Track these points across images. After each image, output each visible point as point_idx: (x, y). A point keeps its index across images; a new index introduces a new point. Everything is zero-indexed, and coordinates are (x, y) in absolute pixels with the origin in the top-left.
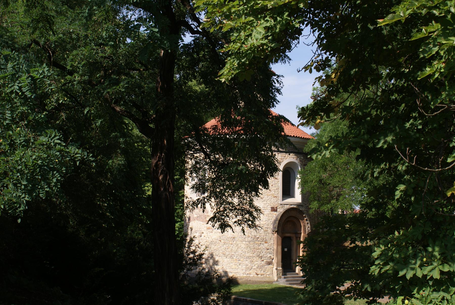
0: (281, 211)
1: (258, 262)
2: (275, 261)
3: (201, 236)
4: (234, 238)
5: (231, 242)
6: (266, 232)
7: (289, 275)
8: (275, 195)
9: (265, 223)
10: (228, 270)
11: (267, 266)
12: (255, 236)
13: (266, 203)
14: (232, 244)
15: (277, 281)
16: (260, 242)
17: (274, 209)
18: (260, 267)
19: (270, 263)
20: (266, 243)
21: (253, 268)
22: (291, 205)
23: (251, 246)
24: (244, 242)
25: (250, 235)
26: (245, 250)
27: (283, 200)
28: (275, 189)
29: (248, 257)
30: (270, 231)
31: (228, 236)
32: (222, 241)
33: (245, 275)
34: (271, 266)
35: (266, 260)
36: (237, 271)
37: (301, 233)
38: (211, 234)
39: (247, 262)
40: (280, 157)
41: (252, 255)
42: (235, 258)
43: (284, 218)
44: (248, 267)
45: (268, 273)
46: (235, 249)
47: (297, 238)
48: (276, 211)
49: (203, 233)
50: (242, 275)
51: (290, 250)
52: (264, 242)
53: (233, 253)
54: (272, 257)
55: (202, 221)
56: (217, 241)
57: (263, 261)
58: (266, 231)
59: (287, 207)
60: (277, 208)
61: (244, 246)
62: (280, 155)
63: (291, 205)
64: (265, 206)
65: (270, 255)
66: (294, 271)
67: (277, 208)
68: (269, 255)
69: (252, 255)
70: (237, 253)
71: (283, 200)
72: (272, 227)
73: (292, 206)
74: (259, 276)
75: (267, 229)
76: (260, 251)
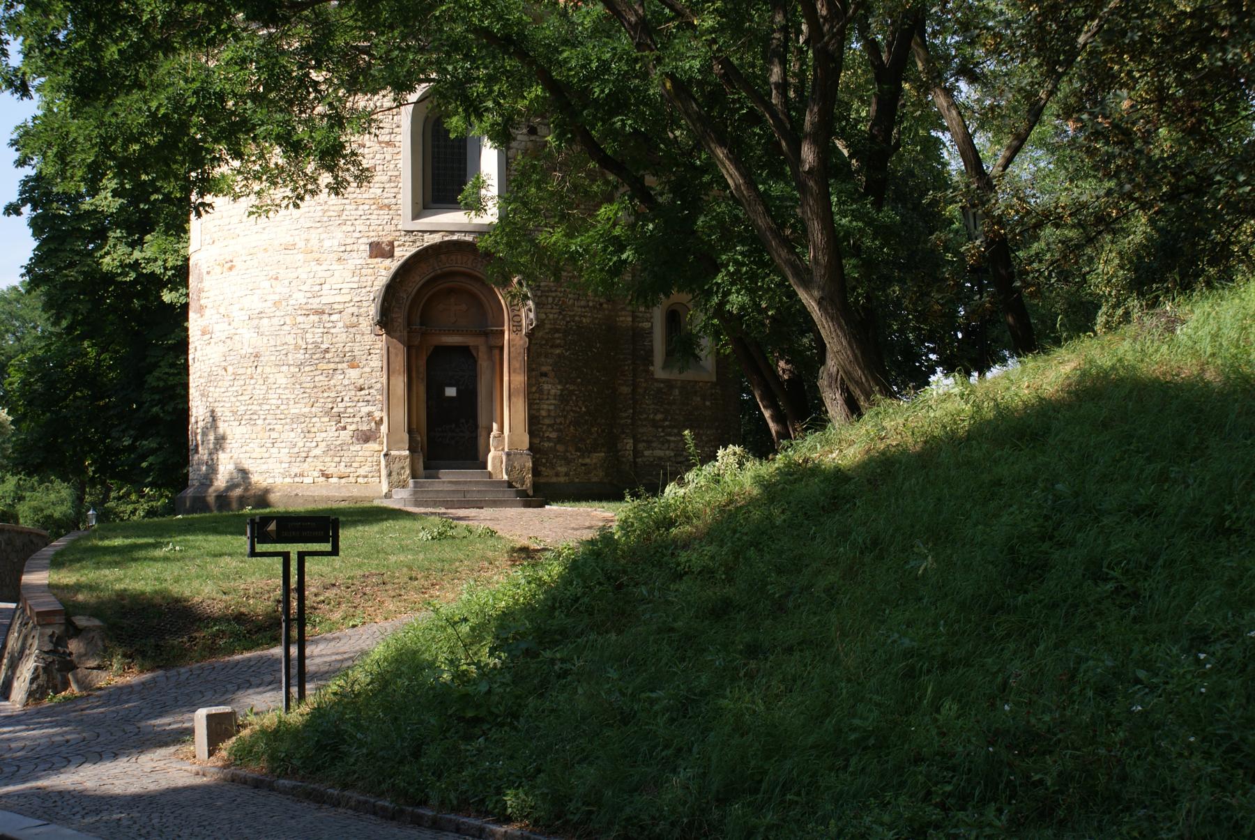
0: (404, 252)
1: (330, 433)
2: (384, 428)
7: (449, 478)
8: (386, 201)
9: (348, 298)
10: (247, 465)
11: (358, 447)
13: (352, 229)
15: (388, 496)
16: (332, 366)
17: (380, 250)
18: (336, 451)
19: (366, 437)
21: (312, 454)
22: (453, 233)
23: (303, 379)
24: (285, 368)
26: (287, 394)
27: (416, 216)
28: (385, 178)
29: (296, 419)
31: (243, 352)
32: (230, 369)
33: (288, 480)
34: (373, 446)
35: (354, 427)
36: (264, 467)
37: (502, 332)
39: (292, 435)
41: (307, 410)
42: (260, 422)
43: (417, 281)
44: (296, 450)
45: (362, 472)
46: (259, 392)
47: (491, 348)
48: (391, 255)
50: (279, 480)
51: (469, 398)
53: (255, 407)
57: (344, 428)
59: (431, 239)
60: (391, 244)
63: (453, 233)
64: (349, 241)
65: (370, 408)
66: (485, 468)
67: (391, 244)
69: (307, 410)
70: (265, 407)
71: (413, 219)
73: (455, 237)
76: (333, 395)
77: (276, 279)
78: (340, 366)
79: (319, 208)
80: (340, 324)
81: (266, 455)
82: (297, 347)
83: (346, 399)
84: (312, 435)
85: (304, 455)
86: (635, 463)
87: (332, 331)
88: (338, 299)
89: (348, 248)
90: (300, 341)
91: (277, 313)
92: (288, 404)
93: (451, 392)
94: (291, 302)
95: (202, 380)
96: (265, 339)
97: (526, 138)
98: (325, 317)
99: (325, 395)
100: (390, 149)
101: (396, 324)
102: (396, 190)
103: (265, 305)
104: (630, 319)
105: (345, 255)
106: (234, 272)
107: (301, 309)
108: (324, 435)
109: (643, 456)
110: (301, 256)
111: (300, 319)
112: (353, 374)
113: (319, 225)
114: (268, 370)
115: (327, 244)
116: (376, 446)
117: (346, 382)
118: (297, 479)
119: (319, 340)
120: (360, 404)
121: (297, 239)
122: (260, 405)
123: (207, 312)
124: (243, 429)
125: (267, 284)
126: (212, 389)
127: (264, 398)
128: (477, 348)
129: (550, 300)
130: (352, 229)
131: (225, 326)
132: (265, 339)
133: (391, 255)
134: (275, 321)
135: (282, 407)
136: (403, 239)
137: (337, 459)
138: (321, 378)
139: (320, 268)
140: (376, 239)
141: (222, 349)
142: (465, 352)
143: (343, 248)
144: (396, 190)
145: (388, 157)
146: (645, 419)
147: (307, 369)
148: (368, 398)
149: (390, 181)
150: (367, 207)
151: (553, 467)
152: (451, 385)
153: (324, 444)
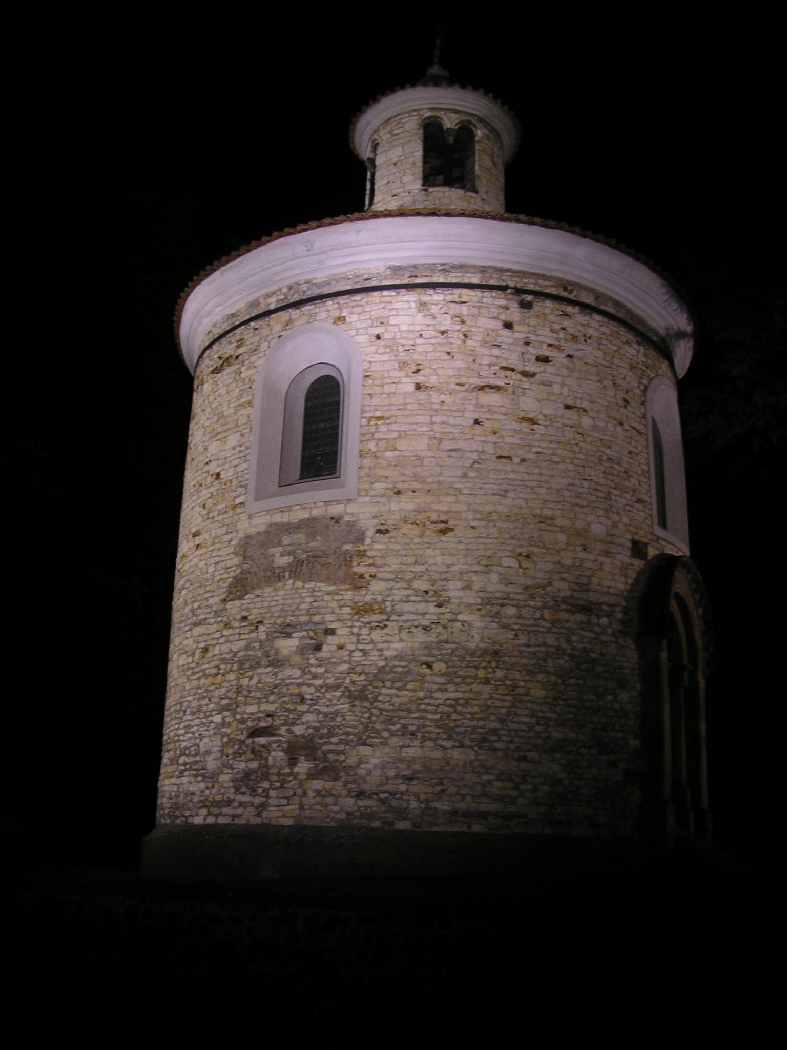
3: (318, 648)
4: (496, 653)
5: (481, 673)
12: (585, 650)
14: (487, 681)
24: (540, 677)
25: (564, 645)
32: (439, 667)
36: (511, 809)
38: (376, 635)
41: (572, 736)
49: (332, 632)
53: (492, 725)
55: (328, 580)
56: (412, 666)
61: (542, 693)
77: (528, 557)
78: (610, 684)
79: (585, 484)
80: (609, 631)
81: (514, 793)
82: (560, 651)
87: (604, 638)
88: (606, 599)
90: (564, 645)
91: (532, 603)
95: (355, 678)
96: (511, 635)
103: (509, 589)
110: (562, 538)
112: (624, 696)
114: (517, 675)
117: (617, 706)
119: (588, 646)
121: (558, 513)
122: (501, 721)
123: (377, 586)
125: (513, 563)
126: (384, 691)
127: (508, 713)
131: (432, 608)
132: (511, 635)
134: (524, 612)
135: (537, 728)
141: (421, 637)
147: (572, 681)
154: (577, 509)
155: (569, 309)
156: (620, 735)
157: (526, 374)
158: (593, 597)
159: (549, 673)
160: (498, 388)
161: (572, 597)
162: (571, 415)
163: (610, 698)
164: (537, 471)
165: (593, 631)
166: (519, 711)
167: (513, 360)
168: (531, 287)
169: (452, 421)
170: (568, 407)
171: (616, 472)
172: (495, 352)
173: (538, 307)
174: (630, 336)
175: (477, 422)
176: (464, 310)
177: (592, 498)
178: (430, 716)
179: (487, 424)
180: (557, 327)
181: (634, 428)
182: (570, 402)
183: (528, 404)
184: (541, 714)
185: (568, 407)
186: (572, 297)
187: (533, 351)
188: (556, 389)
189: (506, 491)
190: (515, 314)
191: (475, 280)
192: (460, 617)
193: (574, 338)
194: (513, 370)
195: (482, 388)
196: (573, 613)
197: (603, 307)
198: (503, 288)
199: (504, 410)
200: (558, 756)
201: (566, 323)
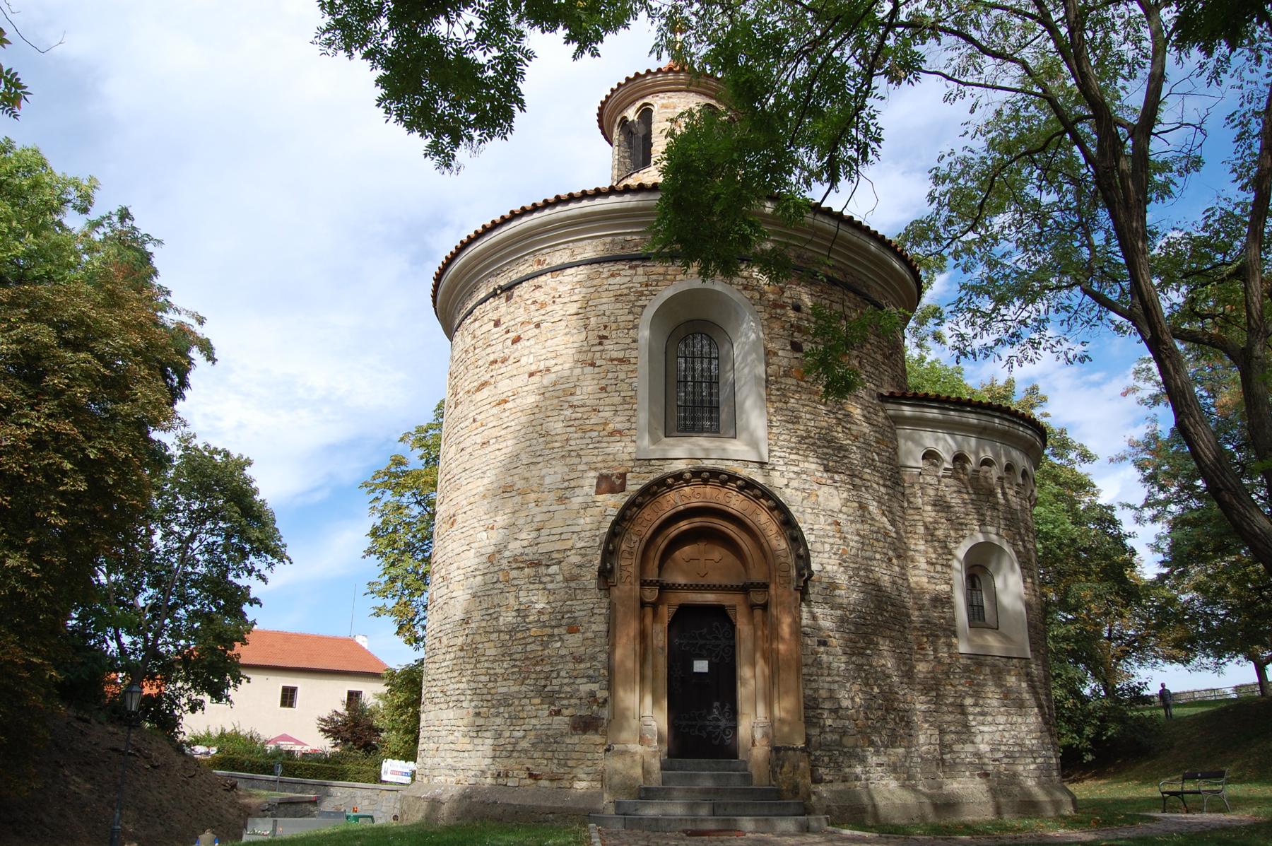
1: (539, 717)
6: (573, 585)
9: (570, 544)
11: (575, 739)
16: (549, 631)
17: (609, 484)
20: (572, 630)
24: (496, 635)
30: (590, 577)
32: (444, 640)
39: (499, 721)
40: (643, 279)
41: (516, 688)
44: (502, 741)
52: (563, 630)
54: (601, 694)
57: (558, 713)
58: (574, 578)
60: (623, 476)
62: (640, 270)
64: (573, 475)
68: (586, 688)
69: (516, 688)
72: (597, 562)
74: (544, 783)
75: (576, 571)
76: (547, 668)
78: (556, 631)
80: (560, 578)
83: (563, 674)
84: (521, 722)
85: (509, 748)
86: (942, 759)
87: (550, 586)
88: (558, 546)
89: (573, 484)
92: (496, 681)
93: (701, 666)
94: (507, 554)
97: (790, 354)
98: (543, 570)
99: (538, 669)
100: (625, 367)
101: (625, 574)
102: (631, 413)
104: (925, 580)
105: (568, 494)
106: (456, 526)
107: (516, 561)
108: (534, 721)
109: (952, 751)
111: (514, 574)
112: (573, 640)
113: (540, 459)
115: (547, 480)
116: (598, 739)
117: (563, 652)
118: (500, 780)
120: (579, 681)
124: (451, 714)
128: (734, 607)
129: (827, 547)
130: (577, 460)
133: (622, 488)
136: (638, 470)
137: (549, 755)
138: (533, 647)
139: (538, 509)
140: (604, 471)
142: (719, 612)
143: (566, 484)
144: (631, 413)
145: (622, 376)
146: (951, 704)
147: (519, 635)
148: (591, 672)
149: (625, 402)
150: (595, 434)
151: (839, 767)
152: (701, 657)
153: (533, 733)
154: (532, 467)
155: (542, 278)
156: (567, 681)
157: (504, 360)
158: (543, 548)
159: (500, 632)
160: (484, 384)
161: (522, 554)
162: (536, 379)
163: (559, 644)
164: (504, 444)
165: (540, 582)
166: (478, 672)
167: (497, 351)
168: (515, 277)
169: (462, 425)
170: (531, 375)
171: (579, 415)
172: (489, 350)
173: (516, 292)
174: (620, 266)
175: (474, 421)
176: (477, 324)
177: (547, 452)
178: (440, 683)
179: (479, 417)
180: (529, 302)
181: (612, 360)
182: (533, 368)
183: (505, 386)
184: (492, 672)
185: (531, 375)
186: (545, 267)
187: (512, 335)
188: (524, 361)
189: (484, 473)
190: (503, 309)
191: (482, 296)
192: (454, 595)
193: (543, 305)
194: (495, 362)
195: (478, 390)
196: (522, 569)
197: (579, 258)
198: (494, 295)
199: (490, 400)
200: (502, 709)
201: (539, 296)
